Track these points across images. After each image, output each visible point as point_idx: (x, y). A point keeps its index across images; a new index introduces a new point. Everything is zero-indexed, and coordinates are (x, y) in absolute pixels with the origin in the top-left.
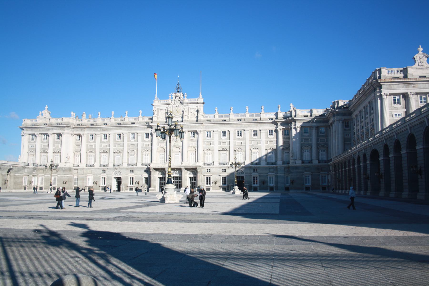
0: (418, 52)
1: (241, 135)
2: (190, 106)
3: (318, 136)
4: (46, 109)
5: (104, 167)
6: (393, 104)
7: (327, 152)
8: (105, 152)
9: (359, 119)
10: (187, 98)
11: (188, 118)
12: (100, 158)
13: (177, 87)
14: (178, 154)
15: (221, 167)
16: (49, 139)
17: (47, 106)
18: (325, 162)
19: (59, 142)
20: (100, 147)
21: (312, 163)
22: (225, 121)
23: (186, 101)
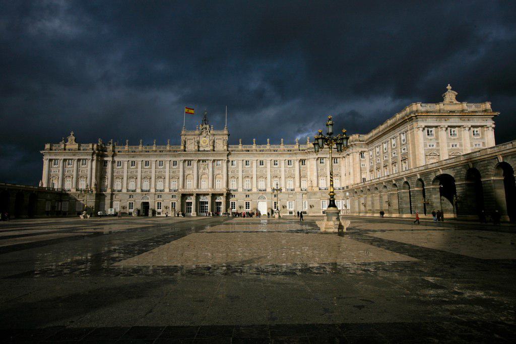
0: (447, 90)
1: (263, 165)
2: (216, 137)
4: (72, 135)
6: (427, 136)
7: (340, 180)
14: (205, 181)
15: (245, 193)
16: (73, 164)
18: (339, 189)
19: (86, 167)
22: (248, 151)
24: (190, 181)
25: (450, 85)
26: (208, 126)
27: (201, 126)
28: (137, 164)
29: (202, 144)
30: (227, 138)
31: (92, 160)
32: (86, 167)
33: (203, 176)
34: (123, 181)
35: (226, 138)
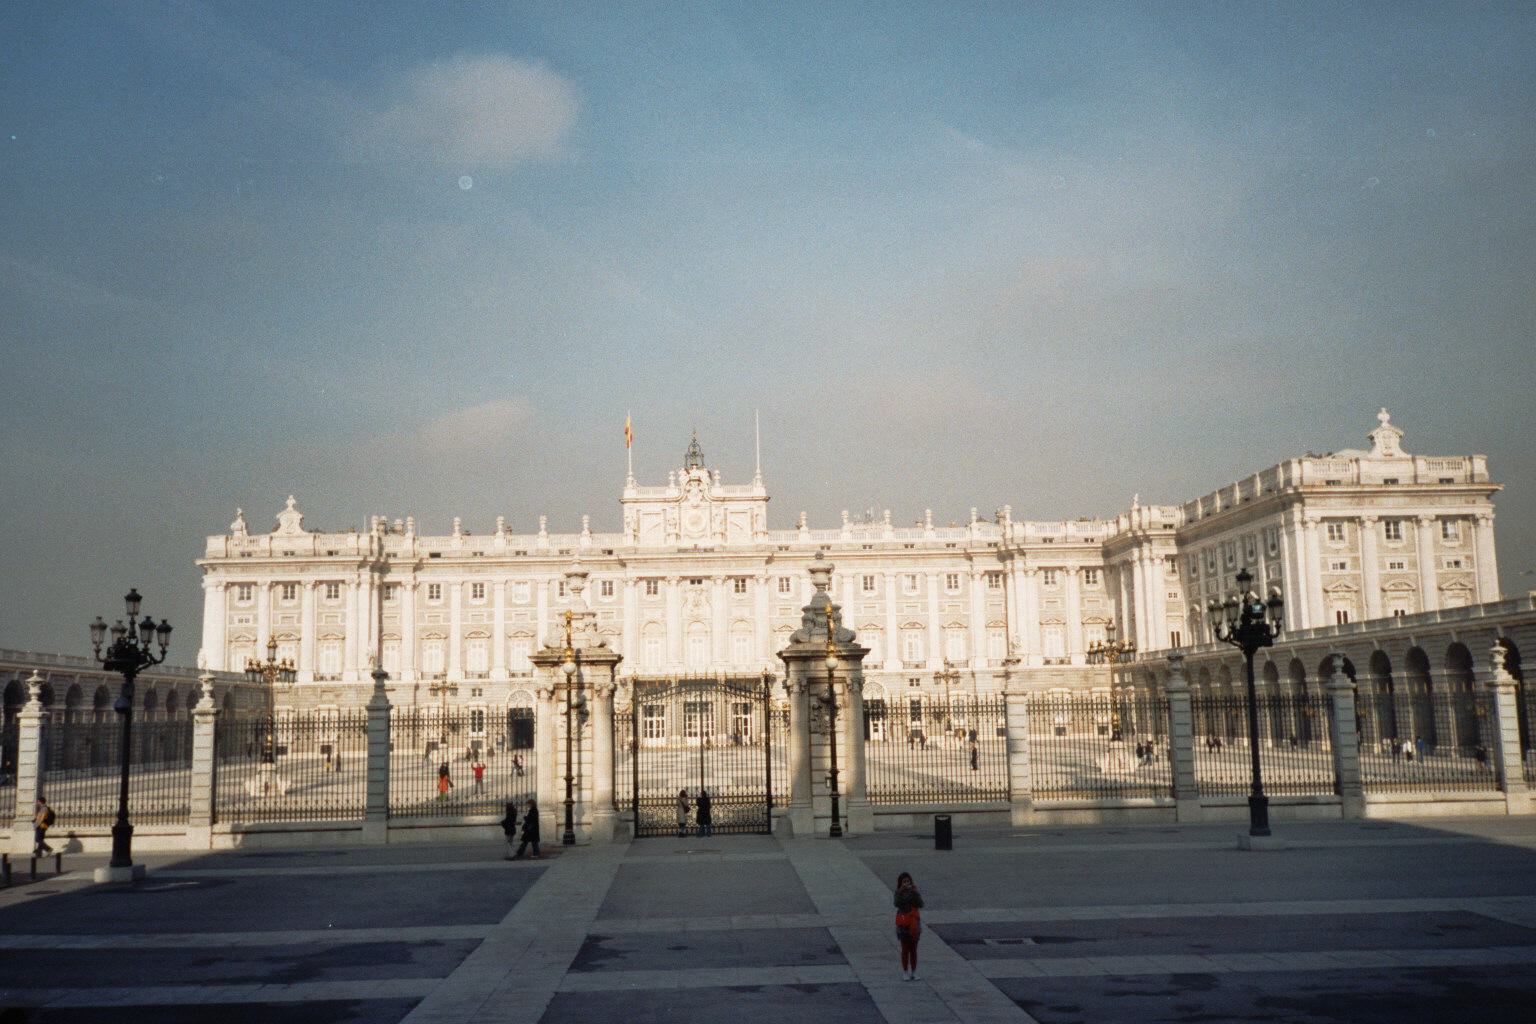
2: (732, 506)
3: (1082, 593)
4: (290, 508)
5: (480, 680)
8: (477, 634)
9: (1220, 563)
10: (723, 483)
11: (726, 541)
12: (464, 653)
13: (691, 450)
16: (300, 598)
17: (291, 497)
19: (340, 607)
20: (462, 620)
21: (1069, 663)
23: (718, 491)
24: (656, 642)
25: (1387, 412)
26: (703, 474)
27: (682, 472)
28: (492, 592)
29: (690, 528)
30: (764, 509)
31: (359, 585)
32: (340, 607)
33: (697, 626)
34: (448, 646)
35: (761, 509)
